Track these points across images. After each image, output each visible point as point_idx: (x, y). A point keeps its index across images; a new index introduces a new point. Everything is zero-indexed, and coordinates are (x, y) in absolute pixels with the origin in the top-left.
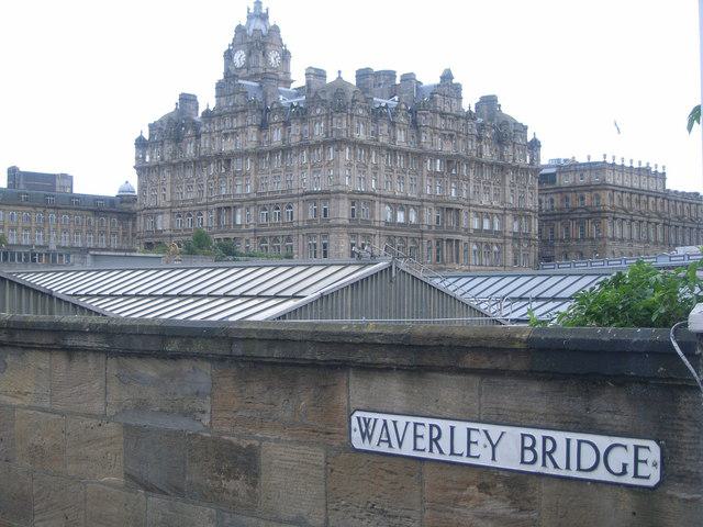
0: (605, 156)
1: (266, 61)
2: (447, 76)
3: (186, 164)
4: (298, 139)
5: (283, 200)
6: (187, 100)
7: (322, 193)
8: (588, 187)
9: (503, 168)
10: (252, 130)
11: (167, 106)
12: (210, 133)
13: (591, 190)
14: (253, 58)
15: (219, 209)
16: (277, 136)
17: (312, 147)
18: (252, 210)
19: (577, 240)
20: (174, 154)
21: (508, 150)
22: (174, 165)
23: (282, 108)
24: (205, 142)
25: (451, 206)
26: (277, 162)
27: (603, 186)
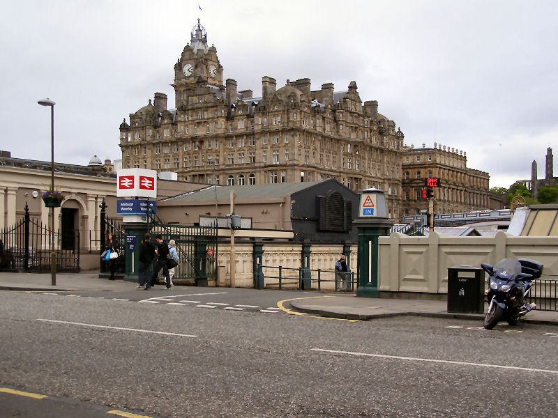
0: (436, 144)
1: (208, 72)
2: (353, 87)
3: (165, 143)
4: (260, 127)
5: (247, 171)
6: (160, 97)
7: (281, 165)
8: (423, 166)
9: (382, 151)
10: (222, 122)
11: (142, 102)
12: (185, 122)
13: (425, 168)
14: (199, 69)
15: (194, 176)
16: (241, 125)
17: (272, 133)
18: (221, 177)
19: (415, 201)
20: (153, 136)
21: (386, 139)
22: (153, 144)
23: (245, 105)
24: (181, 128)
25: (357, 176)
26: (241, 144)
27: (434, 165)
